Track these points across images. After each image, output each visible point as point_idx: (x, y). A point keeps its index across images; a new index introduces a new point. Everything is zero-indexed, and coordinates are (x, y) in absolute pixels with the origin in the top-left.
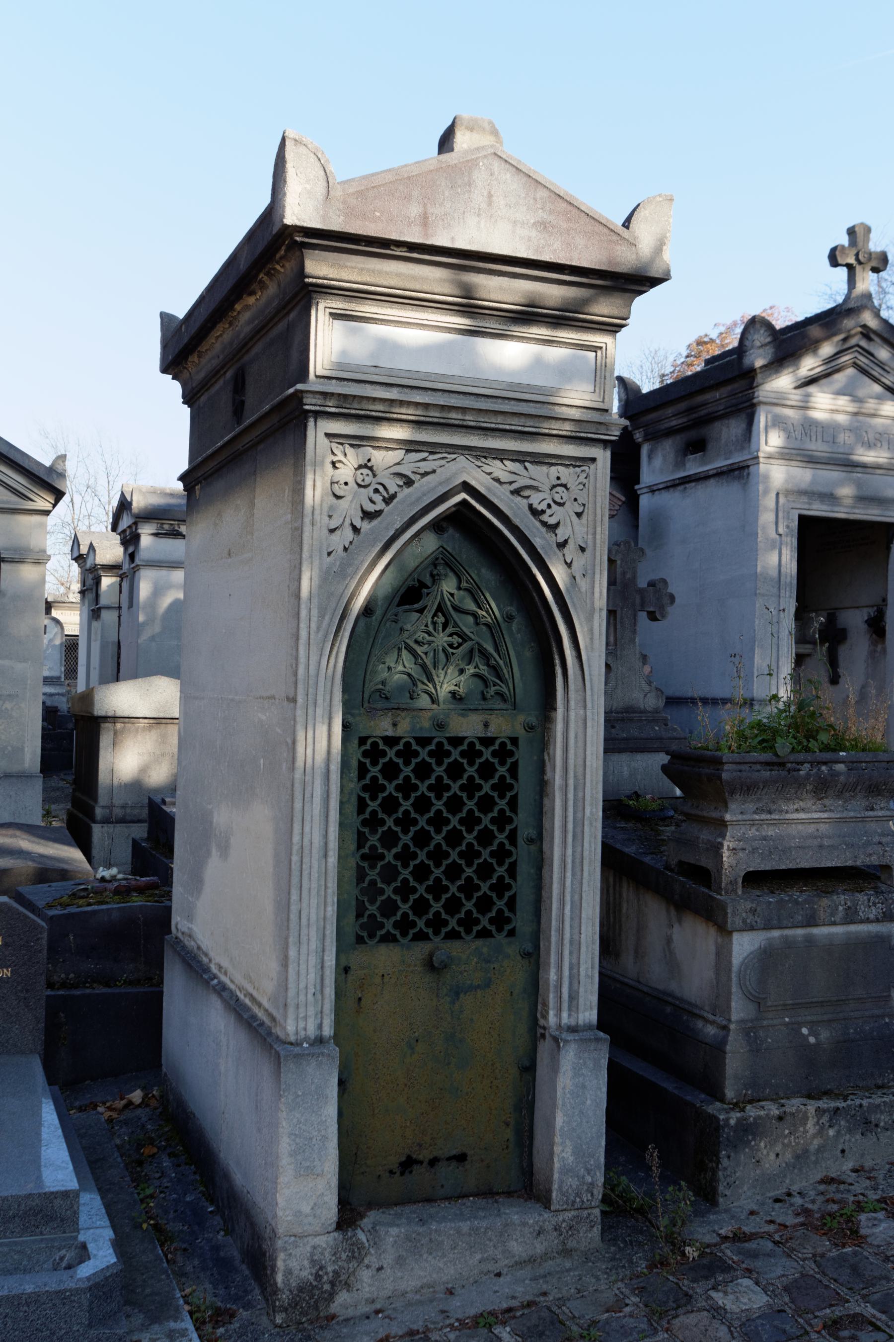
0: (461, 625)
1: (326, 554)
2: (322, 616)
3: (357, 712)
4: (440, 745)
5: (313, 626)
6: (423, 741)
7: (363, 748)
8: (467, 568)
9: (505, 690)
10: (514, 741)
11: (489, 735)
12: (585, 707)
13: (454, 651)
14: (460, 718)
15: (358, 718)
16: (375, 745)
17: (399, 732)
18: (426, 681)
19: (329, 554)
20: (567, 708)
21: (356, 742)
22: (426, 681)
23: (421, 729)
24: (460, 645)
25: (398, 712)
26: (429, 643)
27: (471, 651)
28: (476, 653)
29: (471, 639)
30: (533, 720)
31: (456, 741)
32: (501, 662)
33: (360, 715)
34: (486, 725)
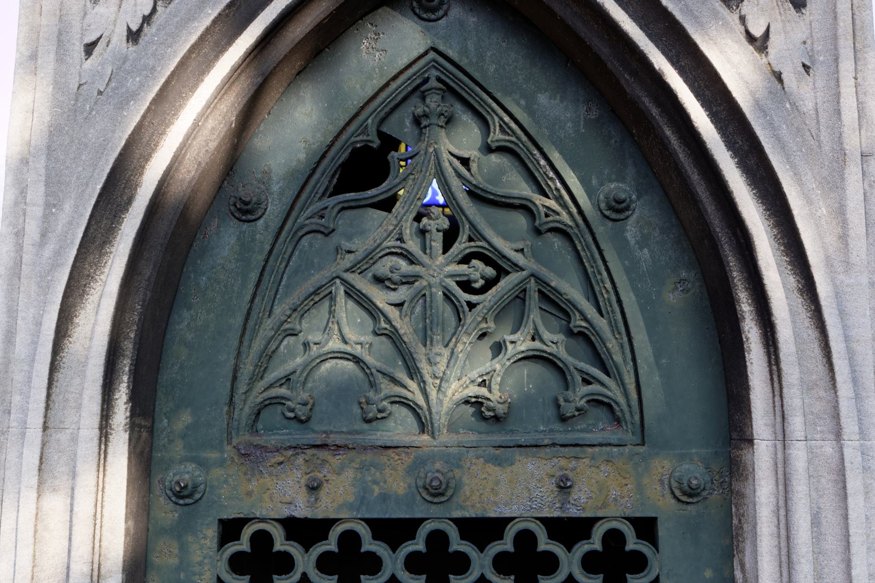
0: (489, 233)
1: (78, 50)
2: (51, 205)
3: (214, 455)
4: (437, 539)
5: (32, 229)
6: (393, 531)
7: (232, 548)
8: (498, 95)
9: (613, 391)
10: (646, 527)
11: (573, 512)
12: (838, 434)
13: (474, 298)
14: (491, 468)
15: (217, 473)
16: (262, 539)
17: (324, 509)
18: (402, 376)
19: (90, 48)
20: (783, 437)
21: (211, 533)
22: (402, 376)
23: (384, 497)
24: (490, 284)
25: (323, 454)
26: (409, 280)
27: (520, 296)
28: (534, 298)
29: (518, 268)
30: (694, 471)
31: (482, 530)
32: (602, 324)
33: (222, 463)
34: (564, 487)
